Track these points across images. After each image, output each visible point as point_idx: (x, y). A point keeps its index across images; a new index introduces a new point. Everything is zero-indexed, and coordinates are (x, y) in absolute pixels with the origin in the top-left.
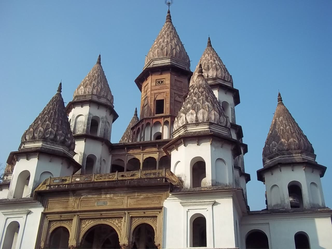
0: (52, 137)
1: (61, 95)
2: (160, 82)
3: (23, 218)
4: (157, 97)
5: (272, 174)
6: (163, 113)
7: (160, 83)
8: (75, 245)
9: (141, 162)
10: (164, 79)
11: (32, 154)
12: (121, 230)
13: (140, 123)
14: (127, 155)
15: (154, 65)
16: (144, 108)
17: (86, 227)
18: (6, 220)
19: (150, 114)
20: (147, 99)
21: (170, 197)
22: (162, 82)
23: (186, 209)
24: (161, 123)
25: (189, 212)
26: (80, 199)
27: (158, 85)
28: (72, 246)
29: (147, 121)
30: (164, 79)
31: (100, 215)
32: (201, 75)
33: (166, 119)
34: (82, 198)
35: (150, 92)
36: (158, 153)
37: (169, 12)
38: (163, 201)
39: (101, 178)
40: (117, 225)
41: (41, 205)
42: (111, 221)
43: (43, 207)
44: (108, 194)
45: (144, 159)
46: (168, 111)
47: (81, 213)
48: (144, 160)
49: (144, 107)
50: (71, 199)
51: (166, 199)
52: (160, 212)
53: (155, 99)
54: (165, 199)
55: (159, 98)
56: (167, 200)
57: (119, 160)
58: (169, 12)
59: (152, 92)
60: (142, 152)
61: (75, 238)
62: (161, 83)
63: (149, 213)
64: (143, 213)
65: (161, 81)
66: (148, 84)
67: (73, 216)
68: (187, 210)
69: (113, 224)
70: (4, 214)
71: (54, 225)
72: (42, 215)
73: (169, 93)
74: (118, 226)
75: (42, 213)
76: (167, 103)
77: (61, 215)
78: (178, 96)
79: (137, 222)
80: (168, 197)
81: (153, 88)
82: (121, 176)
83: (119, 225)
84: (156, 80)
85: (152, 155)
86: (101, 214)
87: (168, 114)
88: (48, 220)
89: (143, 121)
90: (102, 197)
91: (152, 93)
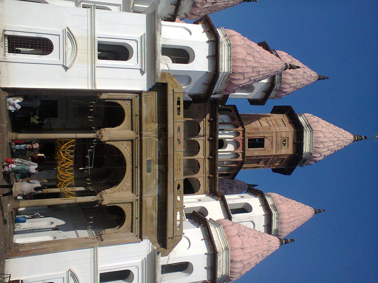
1: (286, 69)
2: (284, 142)
6: (249, 148)
7: (283, 142)
8: (103, 140)
10: (288, 147)
11: (214, 63)
13: (240, 122)
15: (306, 131)
17: (123, 147)
19: (249, 133)
20: (268, 125)
21: (152, 246)
22: (285, 144)
24: (237, 149)
25: (136, 267)
27: (282, 139)
29: (241, 133)
30: (288, 147)
31: (136, 166)
33: (241, 155)
35: (274, 130)
36: (203, 157)
38: (149, 238)
40: (125, 186)
41: (151, 87)
43: (148, 89)
44: (160, 172)
46: (250, 154)
47: (139, 142)
48: (197, 141)
50: (155, 126)
53: (265, 137)
54: (150, 240)
55: (267, 142)
56: (149, 243)
59: (274, 134)
60: (207, 138)
61: (111, 138)
62: (283, 144)
64: (136, 217)
65: (286, 142)
66: (285, 126)
67: (136, 130)
68: (138, 266)
70: (142, 36)
71: (127, 106)
73: (270, 153)
74: (123, 187)
76: (259, 152)
77: (138, 116)
79: (127, 209)
80: (152, 244)
81: (279, 134)
82: (179, 184)
83: (125, 188)
84: (288, 138)
86: (137, 167)
88: (133, 99)
91: (273, 133)
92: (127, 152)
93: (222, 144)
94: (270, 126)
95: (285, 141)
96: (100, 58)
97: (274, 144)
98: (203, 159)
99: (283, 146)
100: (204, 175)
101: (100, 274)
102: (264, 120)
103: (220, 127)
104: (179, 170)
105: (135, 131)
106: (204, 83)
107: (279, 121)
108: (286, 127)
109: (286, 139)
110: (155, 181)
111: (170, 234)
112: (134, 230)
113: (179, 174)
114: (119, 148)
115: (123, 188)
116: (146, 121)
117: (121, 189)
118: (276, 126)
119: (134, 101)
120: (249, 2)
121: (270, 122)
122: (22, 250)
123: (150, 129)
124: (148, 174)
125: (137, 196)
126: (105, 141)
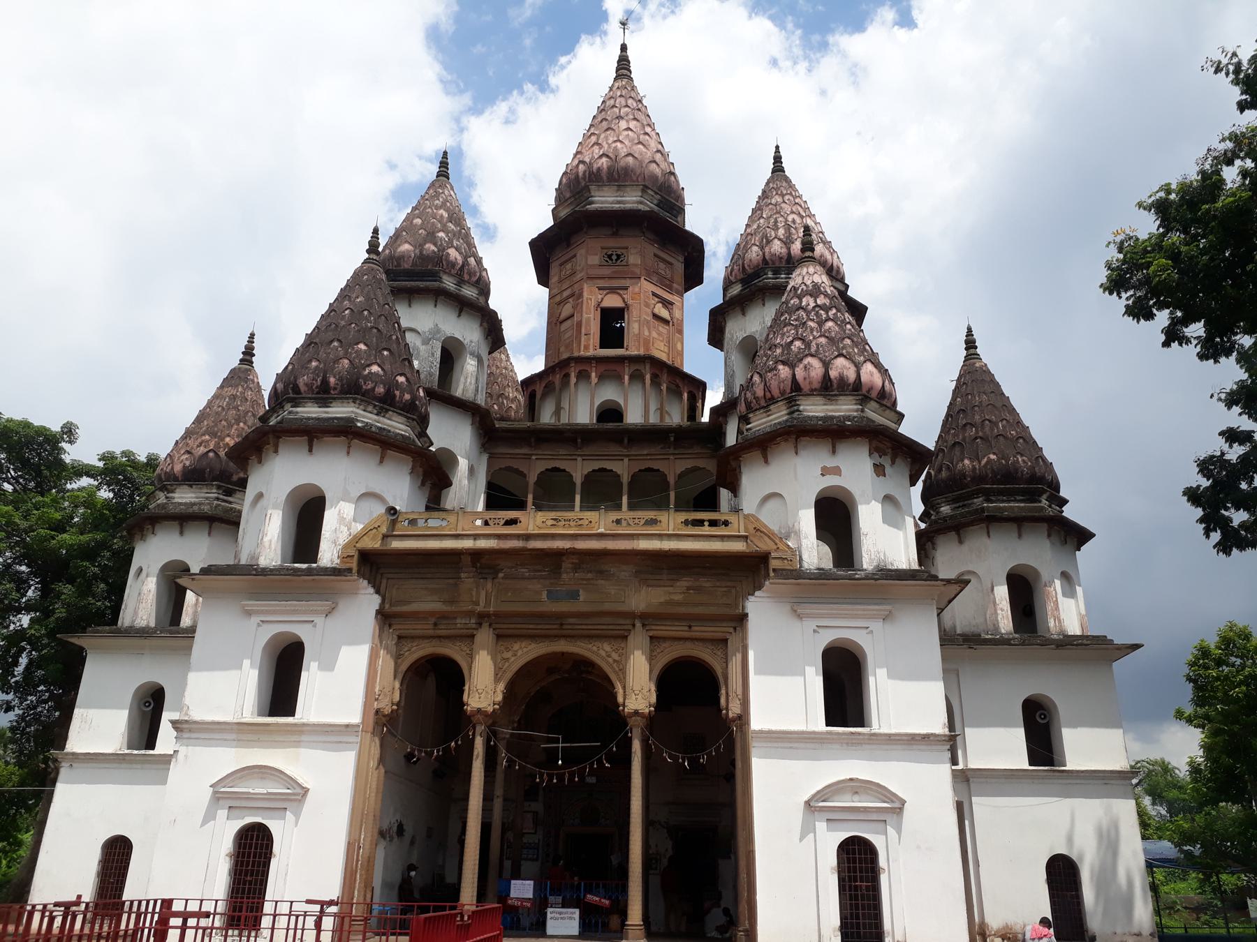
0: (380, 390)
2: (614, 258)
3: (315, 626)
4: (602, 299)
5: (961, 542)
6: (623, 348)
7: (612, 260)
8: (490, 709)
9: (578, 480)
12: (620, 673)
14: (534, 457)
16: (560, 329)
18: (259, 625)
23: (811, 624)
26: (493, 578)
27: (606, 263)
28: (479, 710)
32: (811, 257)
33: (634, 367)
34: (503, 578)
36: (626, 460)
37: (624, 48)
39: (554, 522)
41: (371, 590)
42: (590, 646)
44: (579, 568)
45: (586, 472)
49: (561, 323)
50: (467, 580)
51: (753, 595)
52: (735, 629)
55: (613, 301)
57: (509, 469)
58: (624, 48)
62: (616, 260)
63: (700, 630)
64: (686, 628)
65: (614, 253)
66: (575, 256)
68: (816, 628)
69: (600, 653)
71: (413, 649)
72: (376, 617)
74: (610, 660)
75: (378, 612)
76: (636, 321)
78: (660, 305)
80: (760, 590)
85: (608, 465)
86: (562, 624)
87: (633, 352)
89: (569, 364)
90: (564, 576)
92: (525, 650)
93: (611, 413)
94: (572, 295)
95: (610, 257)
96: (291, 712)
97: (616, 283)
98: (629, 460)
99: (622, 261)
100: (672, 457)
101: (827, 726)
102: (559, 311)
103: (564, 420)
104: (580, 522)
105: (474, 631)
106: (381, 462)
107: (563, 273)
108: (578, 255)
109: (606, 254)
110: (603, 581)
111: (739, 546)
112: (720, 635)
113: (591, 522)
114: (515, 668)
115: (615, 661)
116: (452, 602)
117: (615, 667)
118: (574, 279)
119: (402, 631)
120: (254, 352)
121: (566, 294)
122: (747, 922)
123: (474, 593)
124: (581, 598)
125: (634, 625)
126: (494, 704)
